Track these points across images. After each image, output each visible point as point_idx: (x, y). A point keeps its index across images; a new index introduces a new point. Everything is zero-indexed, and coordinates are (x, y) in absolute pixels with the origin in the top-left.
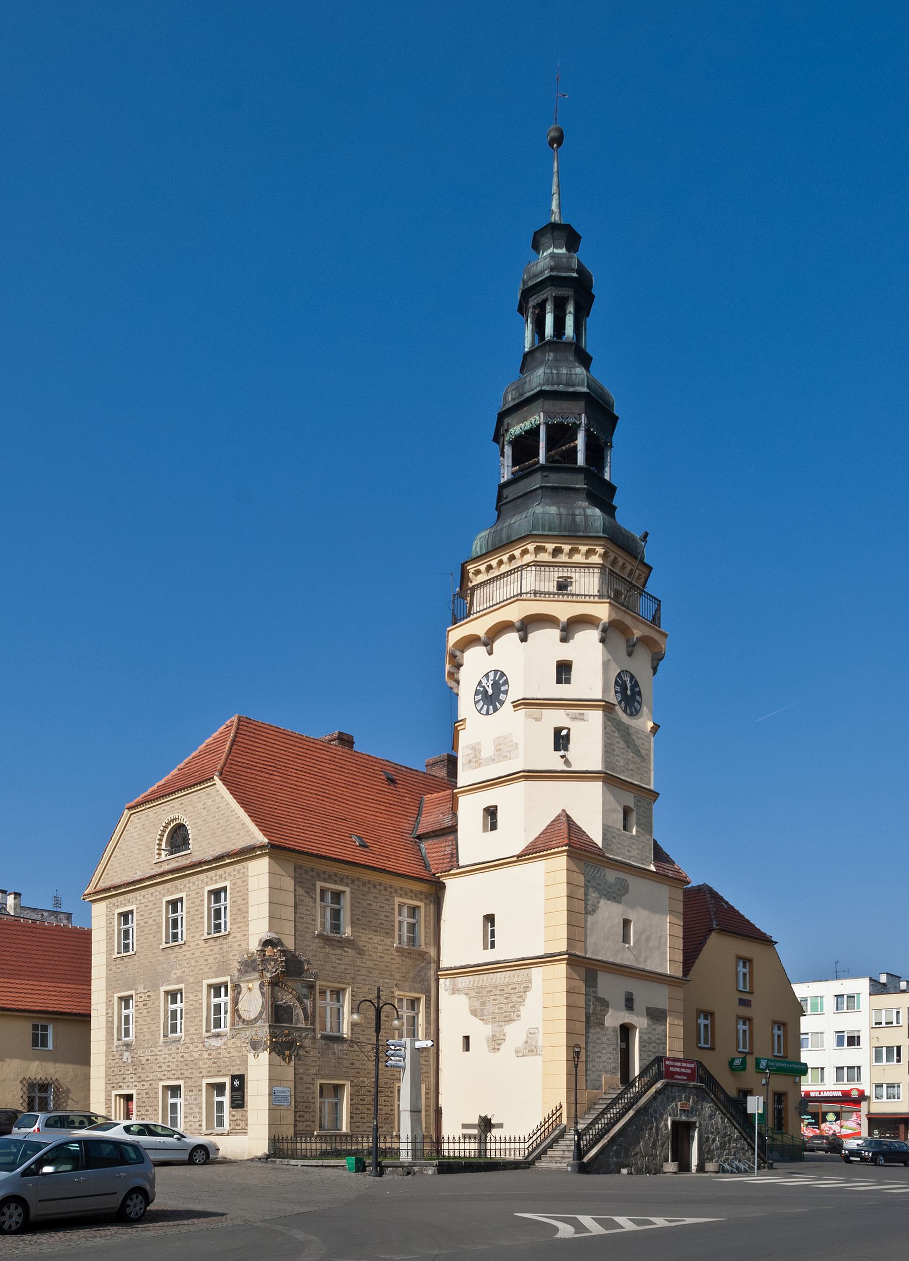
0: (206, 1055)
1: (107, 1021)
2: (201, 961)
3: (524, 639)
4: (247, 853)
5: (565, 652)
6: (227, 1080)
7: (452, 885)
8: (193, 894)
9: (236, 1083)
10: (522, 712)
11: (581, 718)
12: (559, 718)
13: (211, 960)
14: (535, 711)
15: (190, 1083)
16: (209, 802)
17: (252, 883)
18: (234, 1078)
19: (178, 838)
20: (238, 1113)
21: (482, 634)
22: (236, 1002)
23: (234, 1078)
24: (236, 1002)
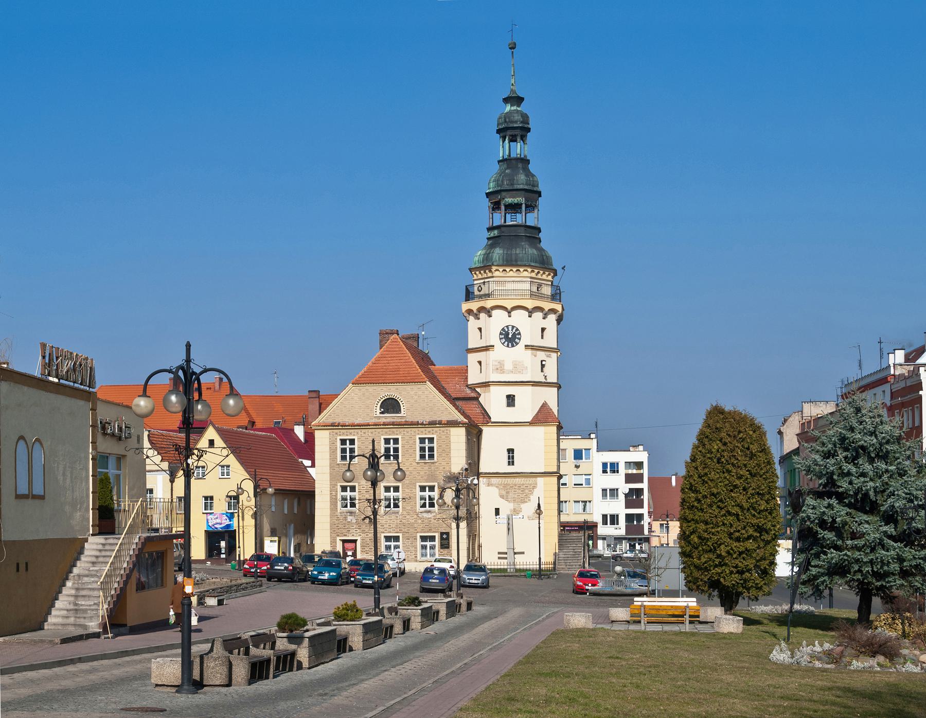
0: (420, 521)
1: (331, 498)
2: (414, 473)
3: (530, 316)
4: (453, 424)
5: (544, 323)
6: (437, 535)
7: (487, 431)
8: (407, 438)
9: (445, 536)
10: (529, 352)
11: (549, 356)
12: (541, 355)
13: (422, 473)
14: (534, 352)
15: (407, 535)
16: (420, 393)
17: (453, 439)
18: (442, 534)
19: (390, 405)
20: (445, 551)
21: (509, 308)
22: (441, 497)
23: (442, 534)
24: (441, 497)
